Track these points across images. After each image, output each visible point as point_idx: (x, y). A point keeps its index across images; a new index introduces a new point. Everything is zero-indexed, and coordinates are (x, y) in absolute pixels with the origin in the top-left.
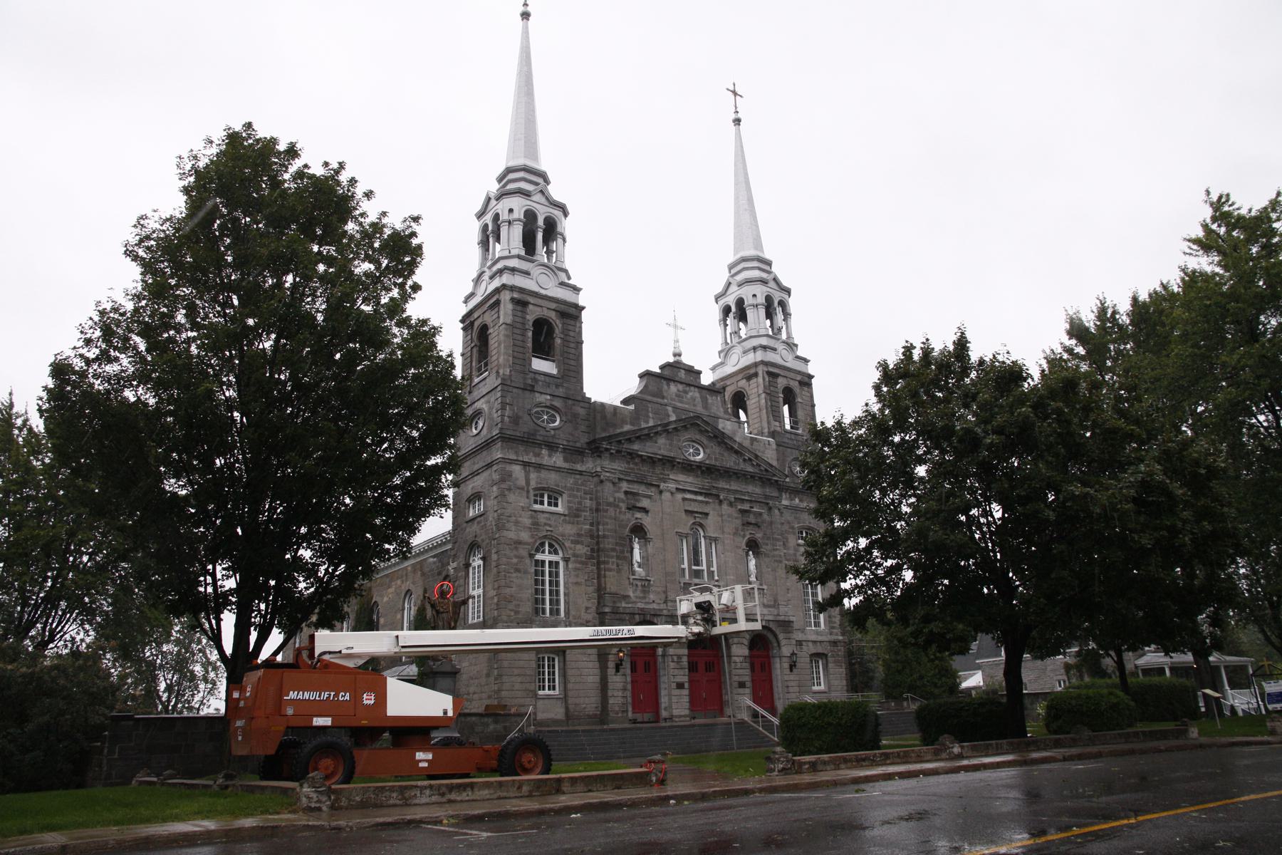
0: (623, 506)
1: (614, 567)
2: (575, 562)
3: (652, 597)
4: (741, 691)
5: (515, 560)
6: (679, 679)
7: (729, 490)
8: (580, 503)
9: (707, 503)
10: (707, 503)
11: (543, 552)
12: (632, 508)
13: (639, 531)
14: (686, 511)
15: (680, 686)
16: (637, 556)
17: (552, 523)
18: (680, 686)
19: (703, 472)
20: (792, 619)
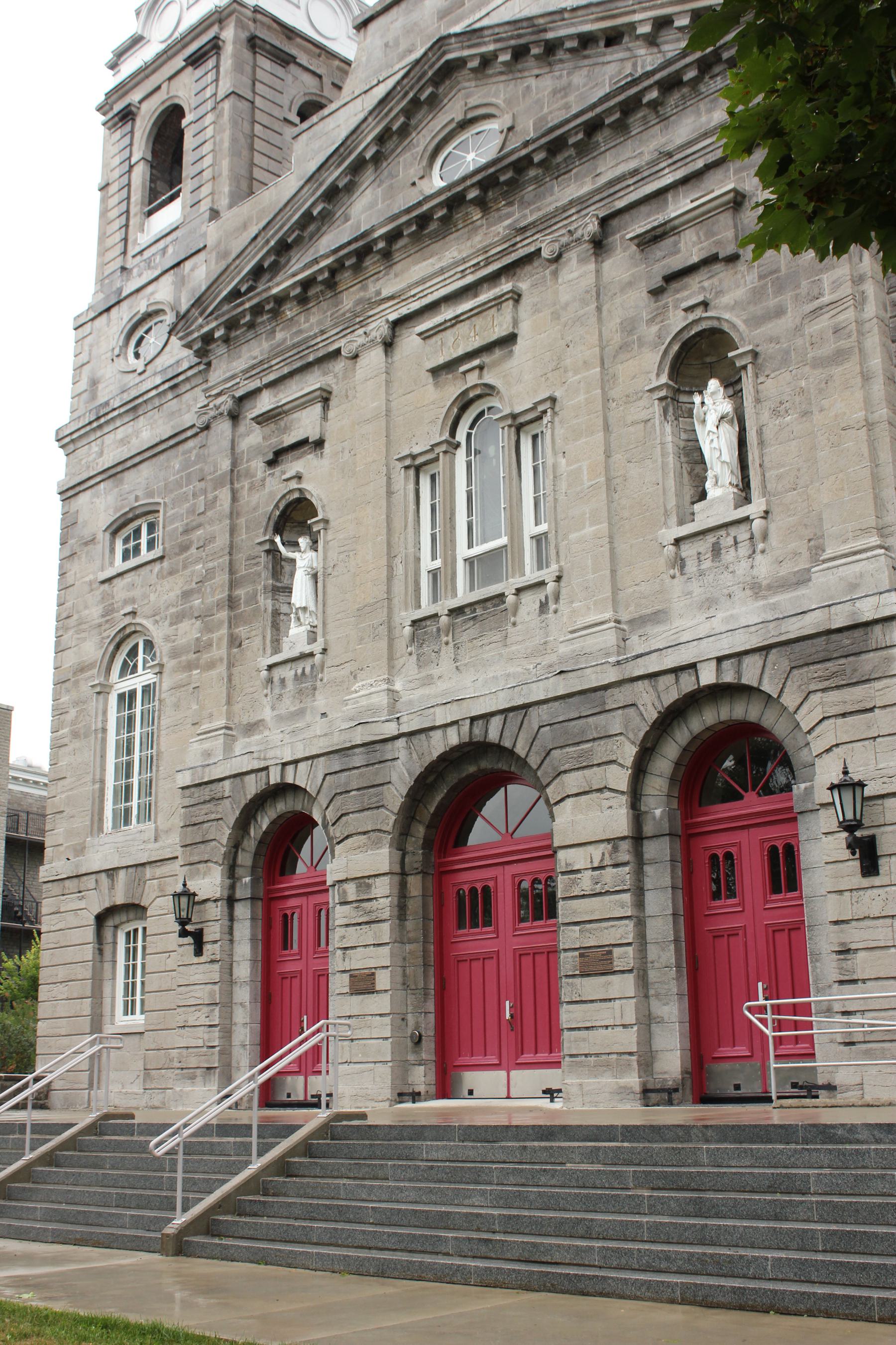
0: (258, 465)
1: (223, 652)
2: (175, 670)
3: (321, 702)
4: (592, 987)
5: (73, 713)
6: (360, 961)
7: (581, 203)
8: (192, 511)
9: (498, 302)
10: (498, 302)
11: (135, 668)
12: (276, 459)
13: (295, 517)
14: (435, 372)
15: (363, 984)
16: (301, 592)
17: (137, 593)
18: (363, 984)
19: (482, 203)
20: (868, 610)
